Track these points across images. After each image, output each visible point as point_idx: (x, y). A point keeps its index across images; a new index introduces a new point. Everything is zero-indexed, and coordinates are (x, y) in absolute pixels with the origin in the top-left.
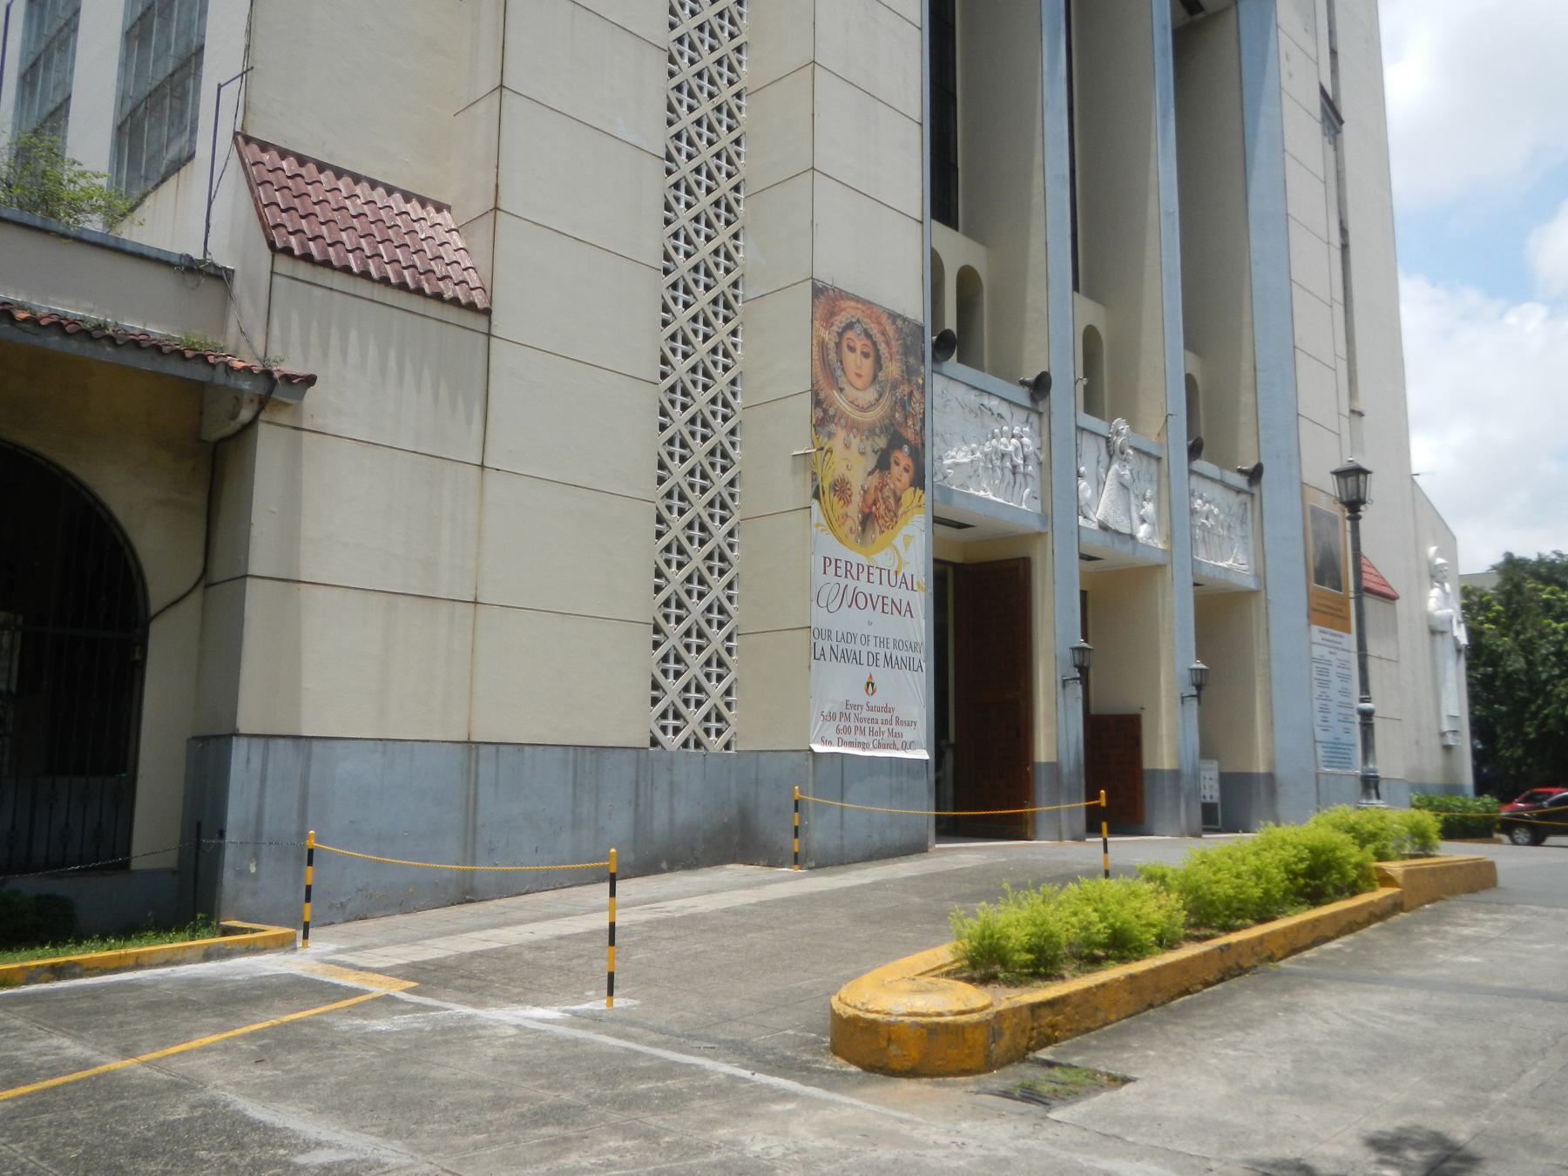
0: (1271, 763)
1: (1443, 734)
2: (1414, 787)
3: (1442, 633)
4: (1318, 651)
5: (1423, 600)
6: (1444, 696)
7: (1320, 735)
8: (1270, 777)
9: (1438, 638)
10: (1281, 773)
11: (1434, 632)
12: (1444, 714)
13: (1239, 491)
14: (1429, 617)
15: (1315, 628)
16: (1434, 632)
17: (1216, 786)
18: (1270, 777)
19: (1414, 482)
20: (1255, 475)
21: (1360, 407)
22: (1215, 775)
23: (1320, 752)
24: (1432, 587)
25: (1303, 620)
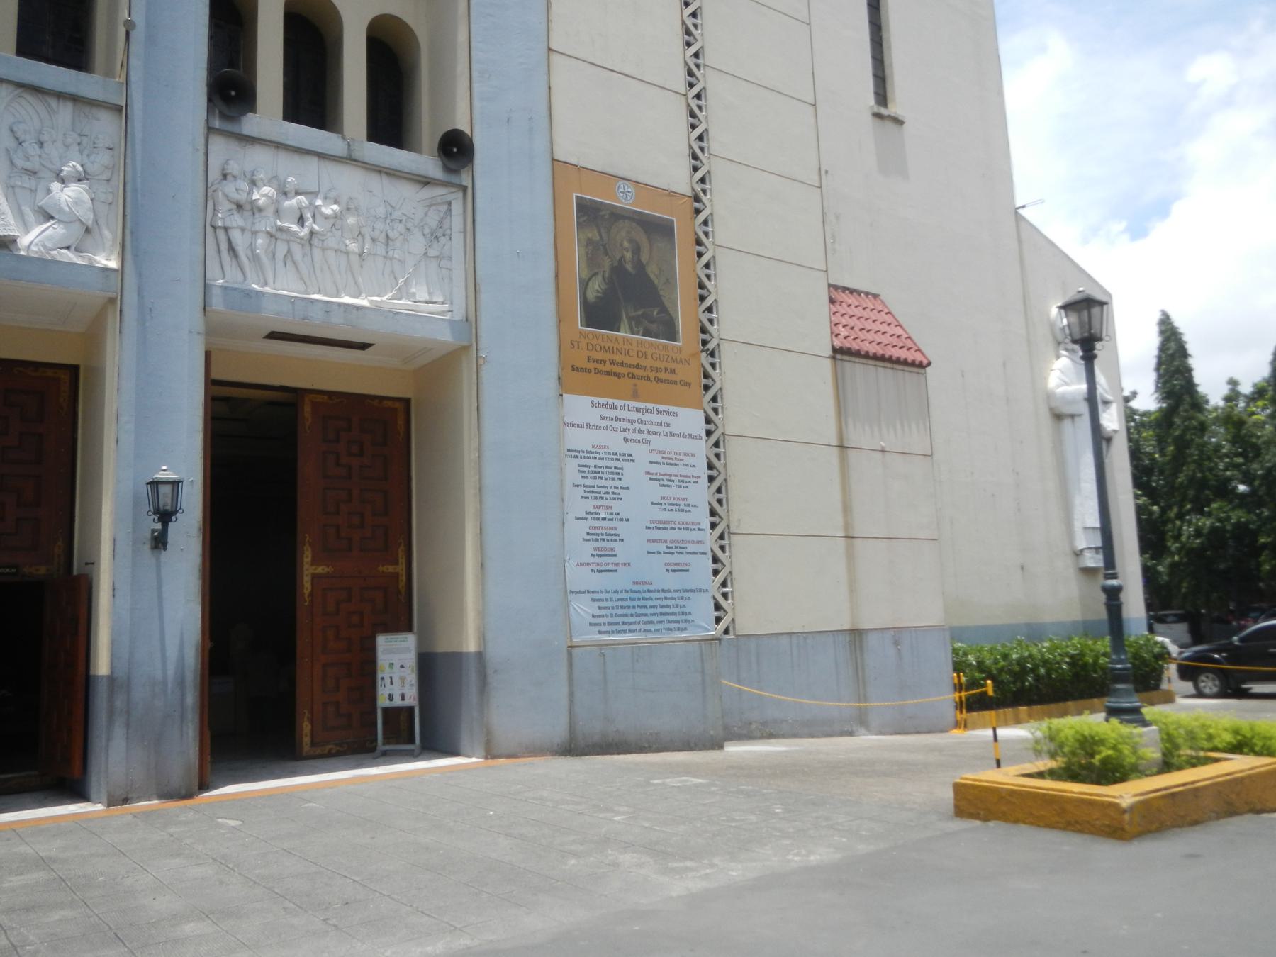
0: (482, 638)
1: (1078, 554)
2: (956, 633)
3: (1072, 416)
4: (580, 440)
5: (1037, 375)
6: (1077, 501)
7: (579, 577)
8: (480, 655)
9: (1067, 423)
10: (495, 653)
11: (1058, 417)
12: (1078, 526)
13: (426, 182)
14: (1049, 396)
15: (580, 406)
16: (1058, 417)
17: (412, 677)
18: (480, 655)
19: (1018, 218)
20: (456, 149)
21: (894, 109)
22: (410, 659)
23: (582, 609)
24: (1058, 357)
25: (553, 383)
